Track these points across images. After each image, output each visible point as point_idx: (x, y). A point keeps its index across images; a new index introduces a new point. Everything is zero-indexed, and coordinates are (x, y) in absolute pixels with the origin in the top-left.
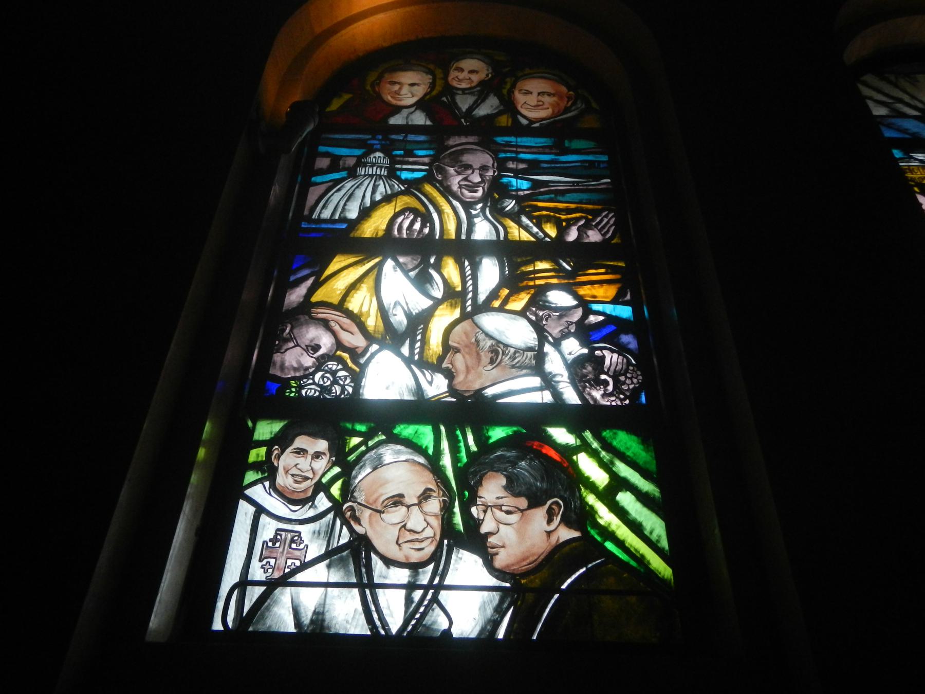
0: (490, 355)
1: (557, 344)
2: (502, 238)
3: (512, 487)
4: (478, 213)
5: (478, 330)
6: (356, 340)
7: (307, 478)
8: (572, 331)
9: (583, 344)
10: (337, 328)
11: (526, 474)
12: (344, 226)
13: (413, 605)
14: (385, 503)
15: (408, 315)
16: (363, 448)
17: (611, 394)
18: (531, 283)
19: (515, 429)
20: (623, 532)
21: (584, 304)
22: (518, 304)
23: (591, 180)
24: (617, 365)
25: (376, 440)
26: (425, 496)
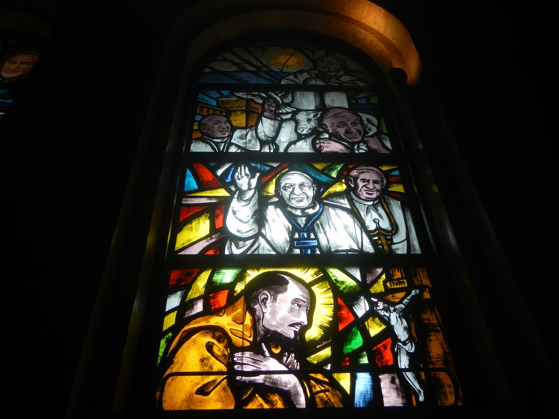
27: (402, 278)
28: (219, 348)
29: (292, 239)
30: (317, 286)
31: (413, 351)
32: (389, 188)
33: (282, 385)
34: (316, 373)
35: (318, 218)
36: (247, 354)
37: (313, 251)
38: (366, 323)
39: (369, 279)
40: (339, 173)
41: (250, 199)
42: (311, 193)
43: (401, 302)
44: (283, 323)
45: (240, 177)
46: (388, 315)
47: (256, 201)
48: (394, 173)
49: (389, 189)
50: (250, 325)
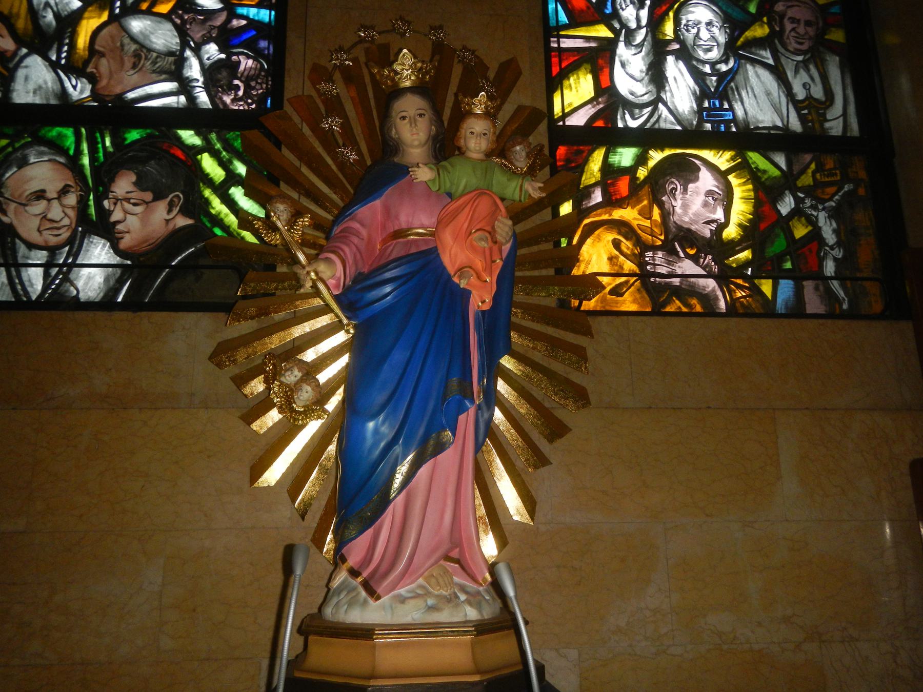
0: (133, 60)
1: (197, 52)
3: (140, 184)
5: (124, 34)
8: (214, 35)
9: (221, 50)
11: (154, 171)
13: (50, 279)
14: (29, 197)
15: (57, 15)
16: (10, 149)
17: (241, 99)
19: (148, 131)
24: (250, 71)
25: (23, 142)
26: (64, 191)
27: (835, 168)
28: (626, 245)
29: (700, 110)
31: (840, 256)
32: (825, 35)
33: (699, 289)
34: (736, 278)
35: (732, 79)
36: (660, 254)
37: (728, 128)
38: (790, 223)
39: (796, 169)
40: (759, 8)
41: (641, 45)
42: (722, 39)
43: (830, 199)
44: (697, 219)
45: (624, 6)
46: (815, 213)
47: (649, 47)
48: (833, 10)
49: (826, 37)
50: (660, 221)
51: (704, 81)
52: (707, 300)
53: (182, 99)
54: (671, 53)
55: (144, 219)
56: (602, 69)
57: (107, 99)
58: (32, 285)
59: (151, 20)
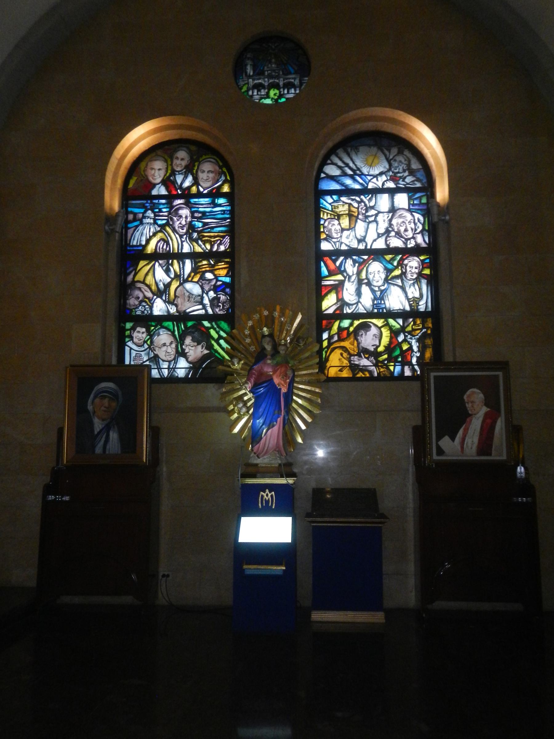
1: (207, 294)
2: (192, 251)
3: (193, 340)
4: (185, 240)
5: (184, 289)
6: (149, 295)
7: (141, 340)
9: (215, 293)
10: (143, 290)
12: (141, 248)
15: (164, 284)
16: (154, 330)
18: (201, 270)
20: (220, 351)
21: (216, 277)
22: (196, 279)
23: (223, 220)
25: (158, 328)
26: (171, 343)
28: (345, 355)
29: (374, 304)
30: (383, 328)
36: (356, 357)
37: (383, 310)
39: (406, 324)
41: (353, 282)
43: (417, 335)
46: (411, 340)
47: (356, 282)
48: (426, 261)
51: (375, 293)
52: (371, 372)
53: (204, 311)
54: (364, 284)
55: (195, 352)
56: (339, 292)
57: (181, 312)
58: (165, 373)
59: (193, 284)
